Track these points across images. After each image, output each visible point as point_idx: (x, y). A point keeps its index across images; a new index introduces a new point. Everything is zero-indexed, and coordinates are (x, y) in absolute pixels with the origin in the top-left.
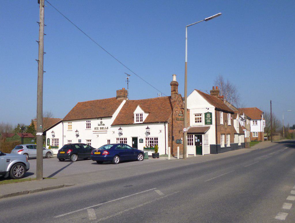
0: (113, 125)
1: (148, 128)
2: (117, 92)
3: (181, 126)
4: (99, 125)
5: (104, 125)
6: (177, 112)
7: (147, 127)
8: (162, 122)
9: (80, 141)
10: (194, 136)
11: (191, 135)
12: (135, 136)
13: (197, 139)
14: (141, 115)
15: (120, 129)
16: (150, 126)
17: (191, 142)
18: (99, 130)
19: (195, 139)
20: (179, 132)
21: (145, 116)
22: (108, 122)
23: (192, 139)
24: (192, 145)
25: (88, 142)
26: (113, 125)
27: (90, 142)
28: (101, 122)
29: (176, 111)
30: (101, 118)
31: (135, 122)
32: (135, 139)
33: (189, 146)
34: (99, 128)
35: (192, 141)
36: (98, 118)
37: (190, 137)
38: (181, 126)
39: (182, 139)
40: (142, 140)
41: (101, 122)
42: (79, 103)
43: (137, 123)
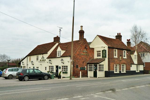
0: (48, 58)
1: (50, 60)
2: (54, 38)
3: (85, 59)
4: (42, 58)
5: (44, 58)
6: (81, 50)
7: (61, 59)
8: (69, 56)
9: (34, 67)
10: (93, 65)
11: (90, 64)
12: (57, 65)
13: (95, 67)
14: (60, 52)
15: (50, 60)
16: (63, 58)
17: (92, 69)
18: (42, 61)
19: (94, 67)
20: (83, 62)
21: (63, 52)
22: (46, 56)
23: (92, 67)
24: (92, 71)
25: (37, 68)
26: (48, 58)
27: (38, 68)
28: (43, 57)
29: (81, 49)
30: (43, 54)
31: (58, 56)
32: (57, 67)
33: (89, 71)
34: (42, 60)
35: (92, 68)
36: (41, 54)
37: (91, 66)
38: (85, 59)
39: (86, 67)
40: (60, 67)
41: (43, 57)
42: (38, 46)
43: (59, 57)
